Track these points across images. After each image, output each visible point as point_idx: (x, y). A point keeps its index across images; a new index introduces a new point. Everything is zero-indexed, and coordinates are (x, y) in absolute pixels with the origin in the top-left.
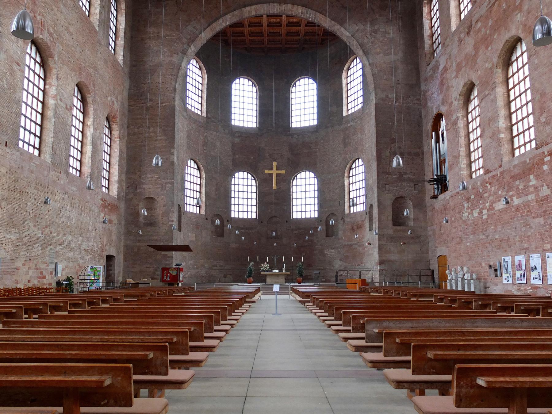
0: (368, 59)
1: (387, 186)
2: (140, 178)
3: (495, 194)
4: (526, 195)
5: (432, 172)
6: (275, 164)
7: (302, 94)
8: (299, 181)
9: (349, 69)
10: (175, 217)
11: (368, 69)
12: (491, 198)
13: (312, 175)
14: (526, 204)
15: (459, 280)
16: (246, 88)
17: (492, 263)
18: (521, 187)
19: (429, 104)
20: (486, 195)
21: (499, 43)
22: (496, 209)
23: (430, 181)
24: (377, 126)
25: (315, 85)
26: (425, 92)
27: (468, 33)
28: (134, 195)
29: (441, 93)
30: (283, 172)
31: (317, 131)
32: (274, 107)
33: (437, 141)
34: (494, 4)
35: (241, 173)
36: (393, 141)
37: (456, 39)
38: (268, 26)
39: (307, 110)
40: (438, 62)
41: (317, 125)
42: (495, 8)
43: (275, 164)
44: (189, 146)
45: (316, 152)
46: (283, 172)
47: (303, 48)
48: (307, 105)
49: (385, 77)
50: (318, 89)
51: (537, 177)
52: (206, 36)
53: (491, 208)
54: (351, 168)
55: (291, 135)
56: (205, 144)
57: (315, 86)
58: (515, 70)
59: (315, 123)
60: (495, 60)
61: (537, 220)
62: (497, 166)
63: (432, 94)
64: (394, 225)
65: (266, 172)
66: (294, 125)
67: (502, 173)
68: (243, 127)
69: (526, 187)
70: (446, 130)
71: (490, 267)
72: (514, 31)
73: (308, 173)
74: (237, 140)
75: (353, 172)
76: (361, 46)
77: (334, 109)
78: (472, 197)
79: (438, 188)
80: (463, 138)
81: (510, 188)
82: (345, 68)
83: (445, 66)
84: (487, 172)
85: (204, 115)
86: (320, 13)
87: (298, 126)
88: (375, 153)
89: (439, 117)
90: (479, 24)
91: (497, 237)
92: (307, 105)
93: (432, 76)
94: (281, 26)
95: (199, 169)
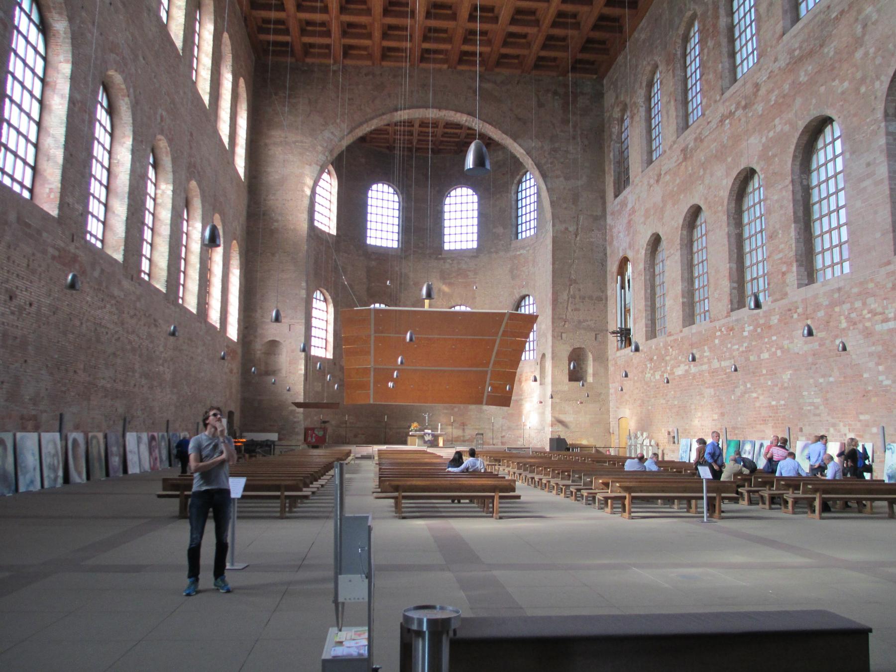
0: (545, 182)
2: (262, 316)
3: (676, 359)
4: (702, 365)
5: (615, 324)
7: (459, 207)
9: (520, 182)
11: (545, 194)
12: (672, 362)
14: (701, 373)
15: (639, 446)
16: (386, 196)
17: (670, 430)
19: (615, 243)
21: (684, 208)
22: (676, 374)
23: (613, 333)
24: (553, 264)
25: (476, 198)
26: (611, 228)
27: (658, 181)
29: (628, 235)
32: (421, 224)
33: (623, 287)
34: (681, 163)
37: (646, 183)
38: (420, 126)
39: (464, 229)
40: (626, 197)
41: (477, 249)
42: (683, 168)
48: (464, 222)
49: (565, 205)
50: (479, 202)
51: (710, 348)
57: (476, 198)
58: (699, 236)
59: (475, 245)
60: (681, 221)
61: (708, 391)
62: (678, 330)
63: (619, 232)
64: (570, 380)
66: (447, 247)
67: (682, 338)
68: (381, 247)
70: (633, 279)
71: (669, 433)
72: (696, 201)
74: (373, 263)
76: (539, 166)
78: (655, 358)
79: (622, 341)
82: (515, 182)
83: (633, 207)
85: (334, 232)
86: (490, 124)
88: (550, 295)
89: (624, 261)
90: (668, 177)
91: (676, 403)
92: (464, 222)
93: (620, 212)
95: (325, 300)
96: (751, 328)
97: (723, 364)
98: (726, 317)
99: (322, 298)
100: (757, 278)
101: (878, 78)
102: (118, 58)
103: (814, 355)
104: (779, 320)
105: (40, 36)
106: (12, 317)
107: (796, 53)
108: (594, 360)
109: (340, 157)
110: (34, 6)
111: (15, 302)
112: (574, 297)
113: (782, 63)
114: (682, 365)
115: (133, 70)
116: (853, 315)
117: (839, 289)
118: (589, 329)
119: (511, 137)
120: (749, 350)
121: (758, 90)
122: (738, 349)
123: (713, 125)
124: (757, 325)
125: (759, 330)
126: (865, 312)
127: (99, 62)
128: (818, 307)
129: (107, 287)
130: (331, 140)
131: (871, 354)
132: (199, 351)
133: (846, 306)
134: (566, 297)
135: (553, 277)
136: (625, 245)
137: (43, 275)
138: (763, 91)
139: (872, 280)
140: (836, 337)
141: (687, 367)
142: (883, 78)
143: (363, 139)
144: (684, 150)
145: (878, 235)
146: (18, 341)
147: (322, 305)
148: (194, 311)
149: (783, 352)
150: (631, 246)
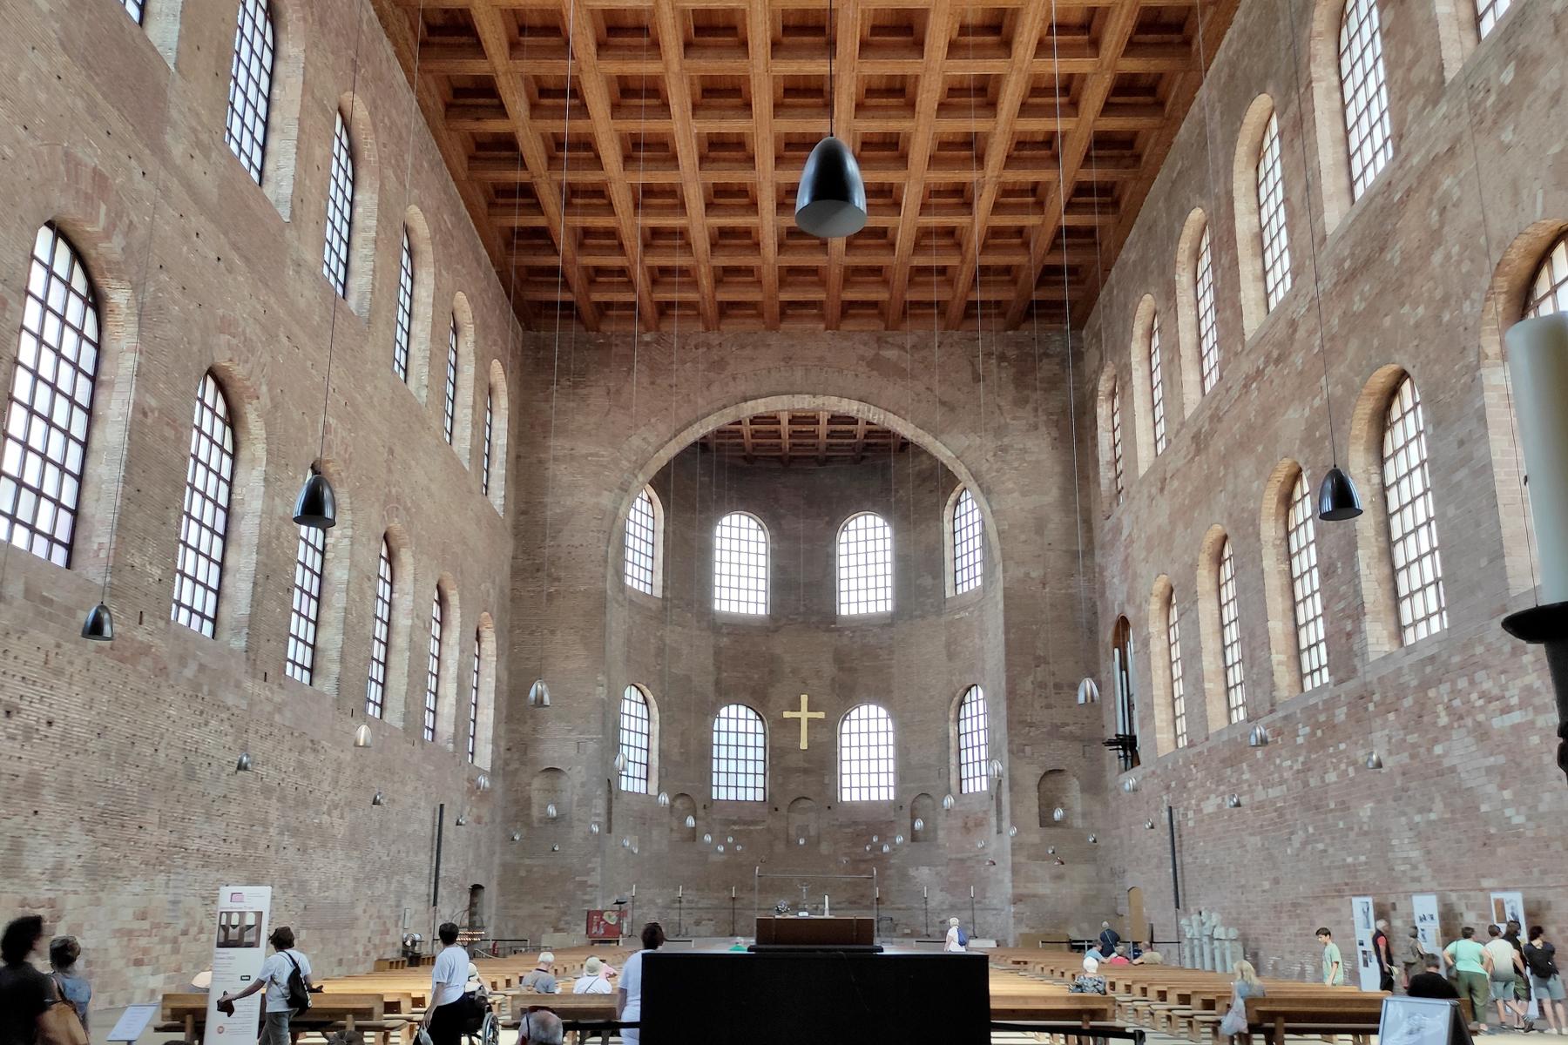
1: (1028, 749)
6: (804, 699)
8: (855, 724)
9: (957, 502)
10: (600, 806)
11: (990, 521)
13: (883, 712)
18: (1234, 781)
20: (1190, 785)
23: (1110, 743)
24: (1007, 632)
28: (523, 763)
30: (821, 715)
31: (890, 625)
33: (1124, 666)
35: (733, 708)
36: (1040, 661)
43: (804, 699)
44: (628, 659)
45: (890, 667)
46: (821, 715)
47: (863, 458)
49: (1023, 537)
51: (1250, 766)
52: (673, 449)
53: (1199, 811)
54: (962, 703)
55: (838, 630)
56: (660, 652)
65: (787, 714)
66: (844, 611)
68: (738, 616)
69: (1240, 782)
73: (873, 708)
74: (725, 641)
75: (967, 711)
76: (976, 476)
77: (928, 581)
79: (1126, 757)
80: (1160, 672)
81: (1220, 781)
82: (950, 502)
84: (1191, 744)
85: (658, 593)
87: (854, 612)
88: (1004, 683)
94: (818, 423)
95: (646, 702)
96: (1308, 729)
97: (1273, 793)
98: (1271, 712)
99: (640, 699)
100: (1316, 644)
101: (1467, 296)
102: (234, 341)
103: (1404, 774)
104: (1348, 715)
105: (90, 313)
106: (9, 744)
107: (1346, 265)
108: (1083, 790)
109: (655, 477)
110: (77, 268)
111: (16, 720)
112: (1042, 685)
113: (1326, 284)
114: (1213, 796)
115: (266, 358)
116: (1457, 703)
117: (1432, 659)
118: (1073, 738)
119: (929, 431)
120: (1307, 768)
121: (1295, 331)
122: (1291, 767)
123: (1235, 393)
124: (1317, 726)
125: (1319, 733)
126: (1474, 696)
127: (195, 349)
128: (1402, 690)
129: (211, 693)
130: (643, 451)
131: (1489, 770)
132: (409, 789)
133: (1445, 688)
134: (1029, 686)
135: (1007, 654)
136: (1121, 597)
137: (77, 677)
138: (1301, 333)
139: (1481, 641)
140: (1436, 741)
141: (1219, 800)
142: (1475, 295)
143: (703, 445)
144: (1196, 438)
145: (1484, 562)
146: (21, 781)
147: (641, 711)
148: (400, 725)
149: (1356, 770)
150: (1130, 599)
